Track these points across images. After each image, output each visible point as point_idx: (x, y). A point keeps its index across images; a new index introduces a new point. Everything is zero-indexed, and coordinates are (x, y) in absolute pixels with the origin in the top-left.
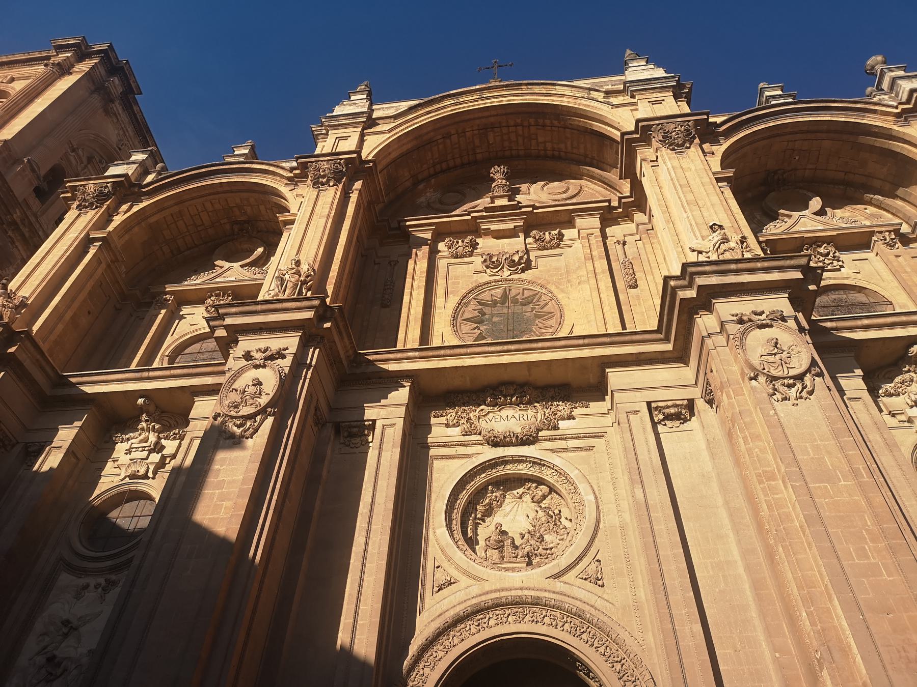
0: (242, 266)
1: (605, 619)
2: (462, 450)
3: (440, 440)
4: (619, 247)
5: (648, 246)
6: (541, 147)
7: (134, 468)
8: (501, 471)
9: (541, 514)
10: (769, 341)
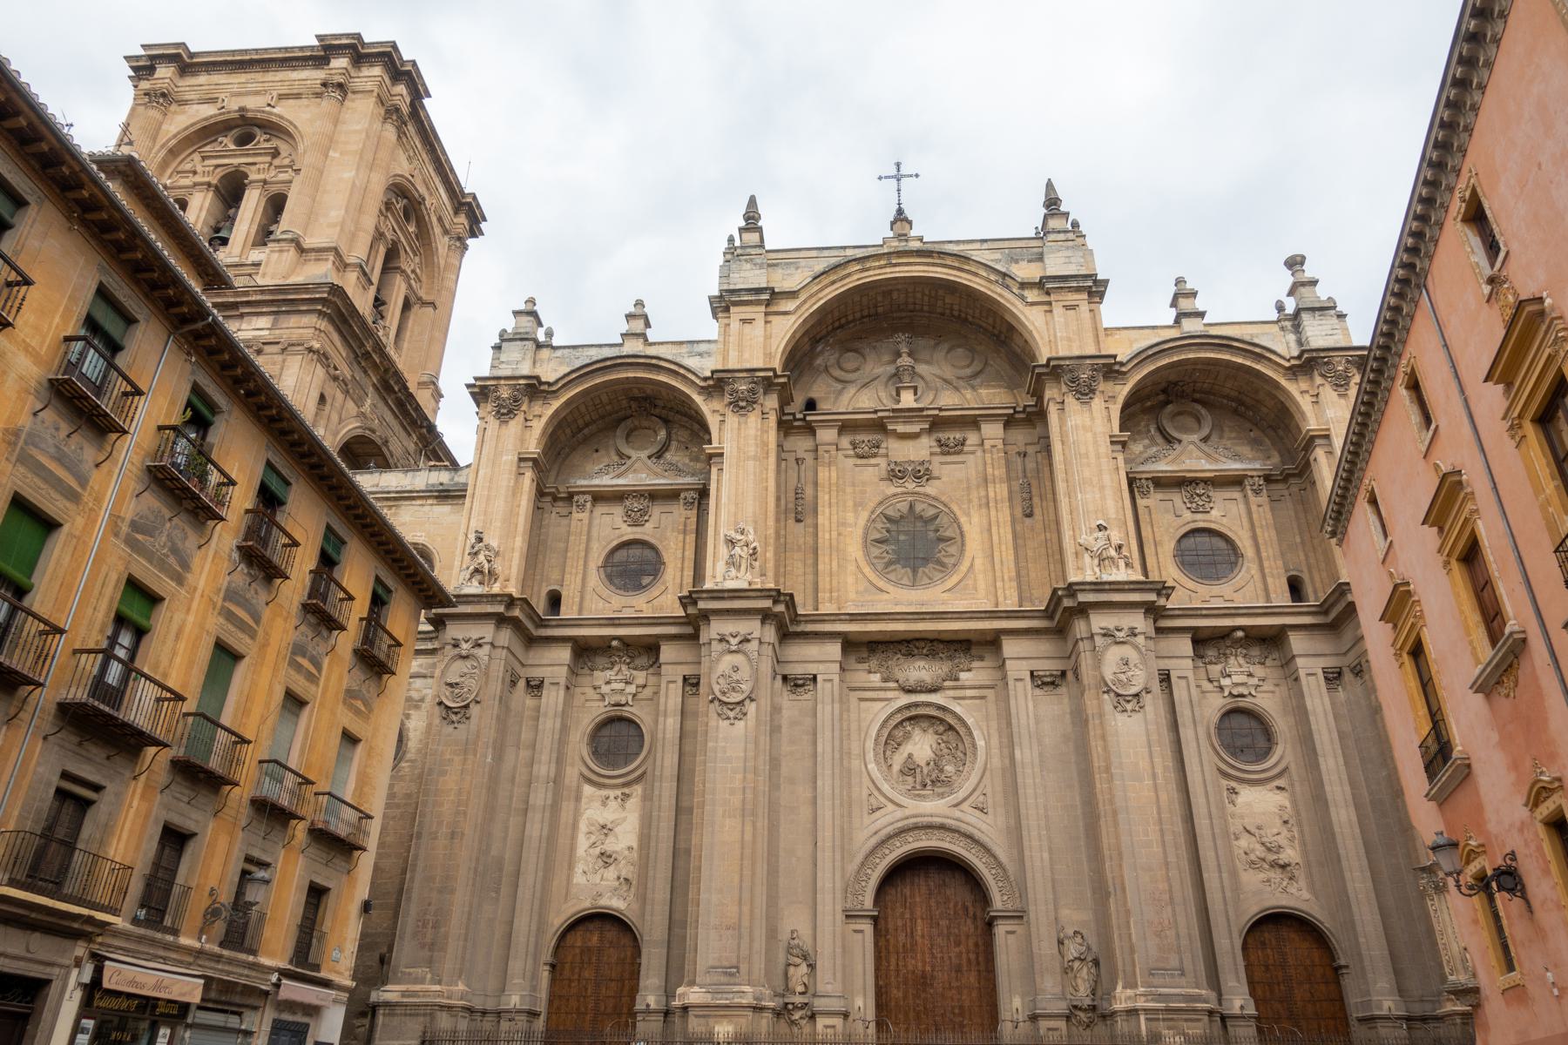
2: (882, 694)
5: (1047, 469)
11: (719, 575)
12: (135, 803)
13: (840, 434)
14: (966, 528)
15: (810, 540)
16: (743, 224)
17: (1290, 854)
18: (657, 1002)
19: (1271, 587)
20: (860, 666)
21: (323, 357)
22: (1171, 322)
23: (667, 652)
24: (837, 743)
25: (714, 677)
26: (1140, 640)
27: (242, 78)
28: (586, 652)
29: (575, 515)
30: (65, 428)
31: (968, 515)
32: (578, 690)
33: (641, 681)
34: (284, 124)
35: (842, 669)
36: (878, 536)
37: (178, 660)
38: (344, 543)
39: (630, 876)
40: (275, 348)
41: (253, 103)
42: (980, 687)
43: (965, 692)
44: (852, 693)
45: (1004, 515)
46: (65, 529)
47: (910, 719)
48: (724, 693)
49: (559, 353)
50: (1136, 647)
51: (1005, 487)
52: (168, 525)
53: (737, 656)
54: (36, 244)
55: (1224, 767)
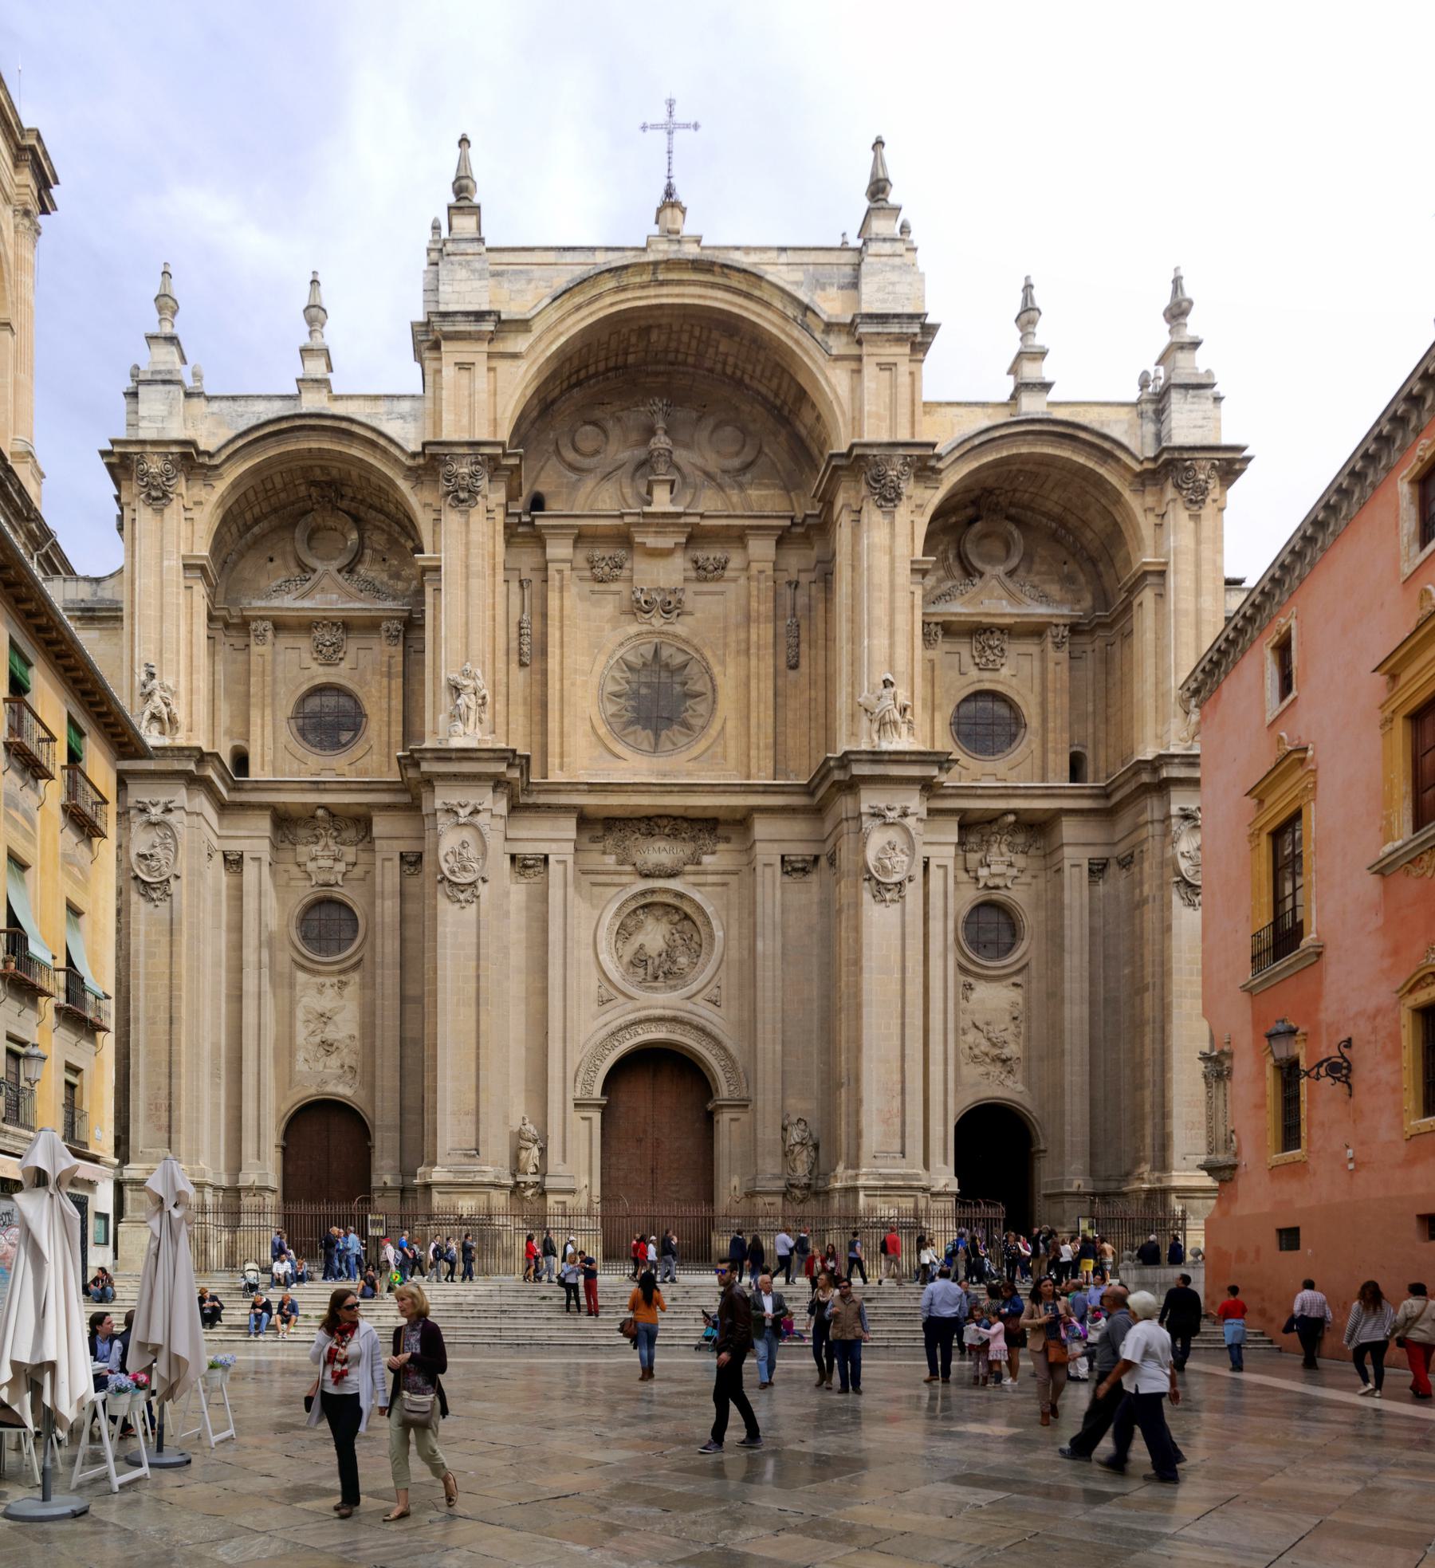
3: (599, 868)
6: (720, 358)
7: (323, 877)
17: (1013, 1050)
19: (1051, 765)
20: (595, 846)
33: (351, 858)
39: (353, 1064)
42: (724, 873)
43: (705, 880)
55: (964, 962)
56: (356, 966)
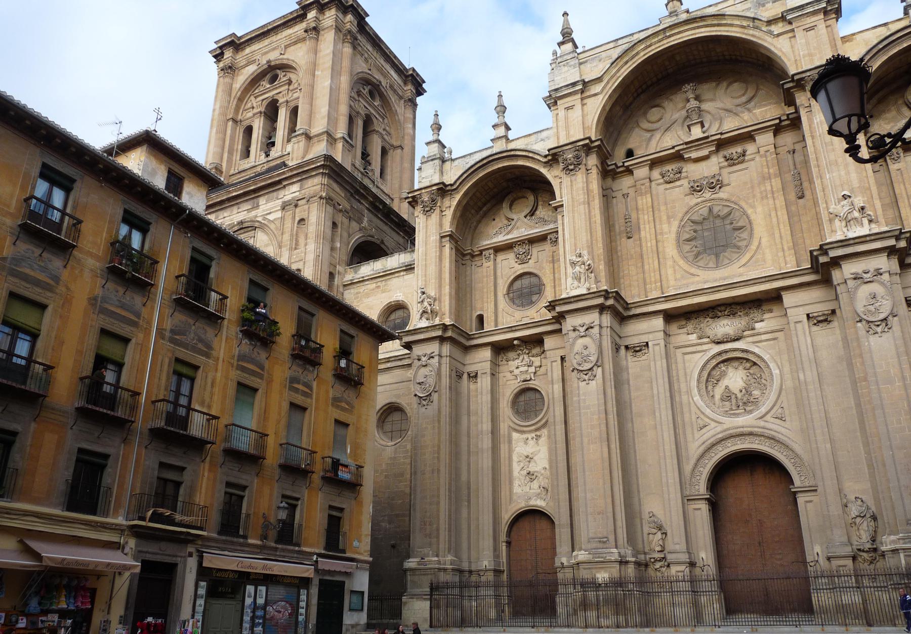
0: (525, 217)
1: (786, 439)
2: (699, 348)
4: (790, 156)
7: (523, 377)
8: (725, 357)
9: (750, 378)
10: (870, 295)
11: (571, 287)
12: (206, 474)
13: (651, 168)
14: (752, 217)
15: (638, 249)
16: (560, 39)
18: (568, 561)
21: (329, 200)
22: (902, 15)
23: (549, 342)
24: (667, 386)
25: (572, 355)
26: (886, 277)
27: (266, 42)
28: (501, 349)
29: (485, 265)
30: (121, 290)
31: (753, 207)
32: (501, 375)
33: (537, 363)
34: (290, 63)
35: (667, 334)
36: (687, 236)
37: (215, 398)
38: (313, 315)
39: (546, 486)
40: (303, 202)
41: (274, 56)
44: (678, 350)
45: (780, 202)
46: (133, 341)
47: (723, 361)
48: (580, 365)
49: (456, 162)
50: (882, 284)
51: (778, 180)
52: (193, 327)
53: (585, 337)
54: (85, 200)
56: (545, 425)
